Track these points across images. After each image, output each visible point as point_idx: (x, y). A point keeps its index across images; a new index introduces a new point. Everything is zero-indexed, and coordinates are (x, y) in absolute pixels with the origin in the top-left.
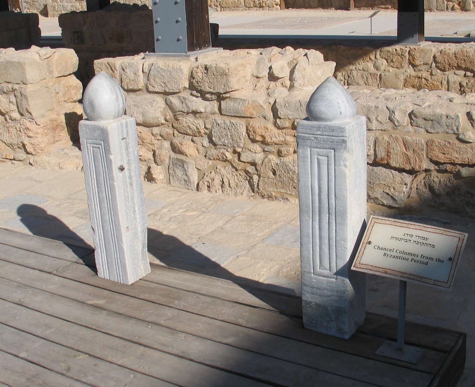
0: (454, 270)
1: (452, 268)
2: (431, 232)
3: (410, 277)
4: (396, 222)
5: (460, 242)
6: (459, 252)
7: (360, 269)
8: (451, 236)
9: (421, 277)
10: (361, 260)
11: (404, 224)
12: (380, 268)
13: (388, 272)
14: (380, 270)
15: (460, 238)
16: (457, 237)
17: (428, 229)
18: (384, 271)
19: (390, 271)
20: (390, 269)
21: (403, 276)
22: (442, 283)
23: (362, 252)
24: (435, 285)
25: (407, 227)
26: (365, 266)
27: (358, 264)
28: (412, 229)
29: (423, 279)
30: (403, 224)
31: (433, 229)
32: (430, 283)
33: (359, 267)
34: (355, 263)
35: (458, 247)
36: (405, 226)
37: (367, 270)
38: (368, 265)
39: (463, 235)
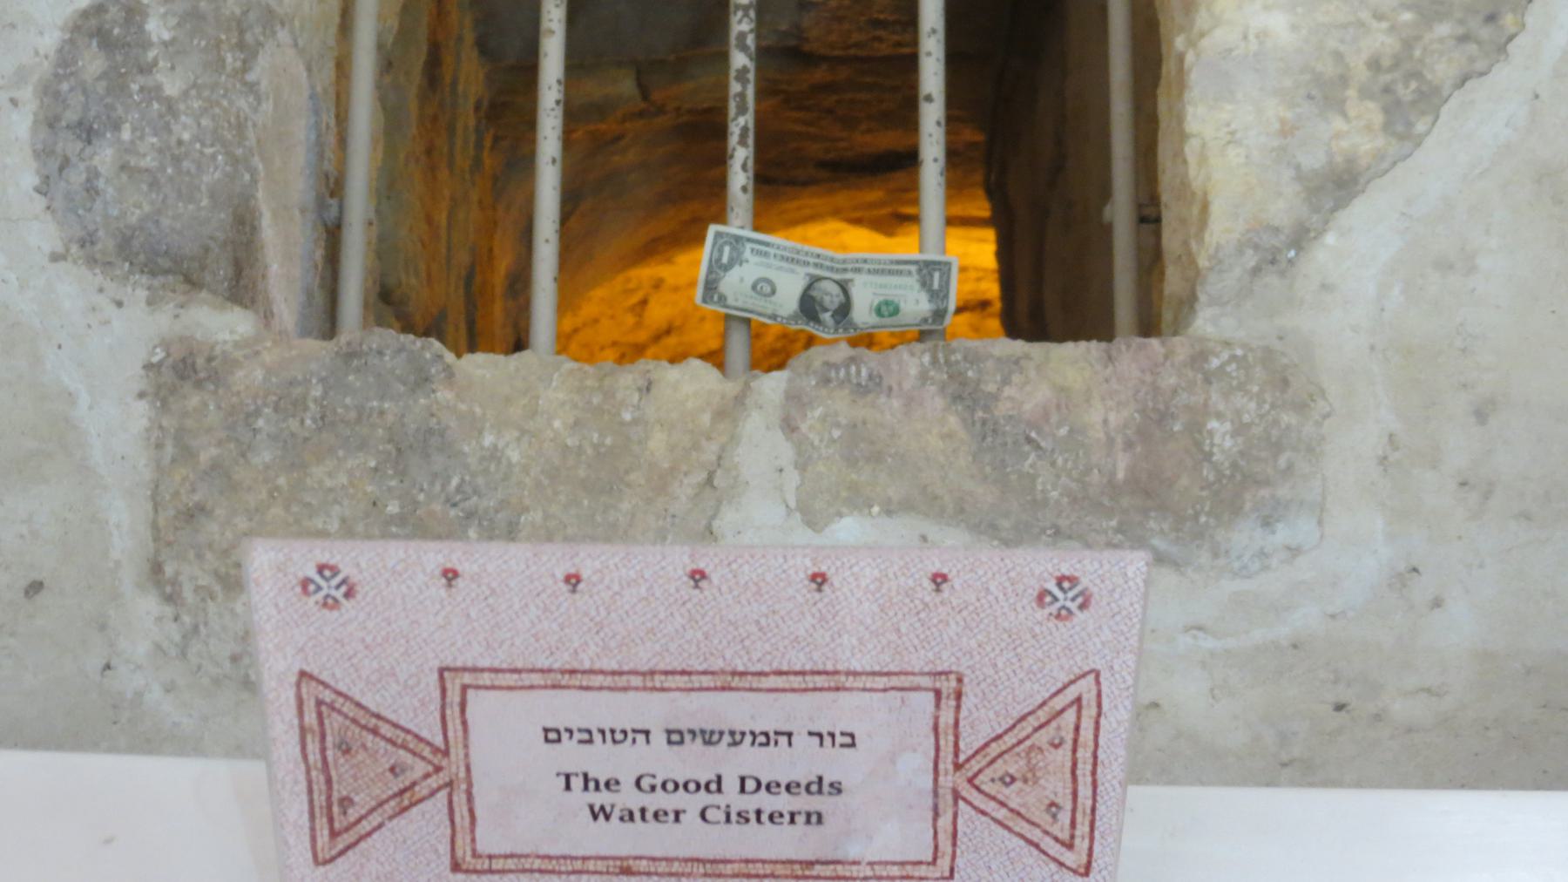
8: (893, 688)
9: (801, 863)
10: (473, 840)
19: (644, 862)
20: (640, 858)
25: (649, 684)
30: (625, 678)
31: (792, 678)
39: (952, 677)
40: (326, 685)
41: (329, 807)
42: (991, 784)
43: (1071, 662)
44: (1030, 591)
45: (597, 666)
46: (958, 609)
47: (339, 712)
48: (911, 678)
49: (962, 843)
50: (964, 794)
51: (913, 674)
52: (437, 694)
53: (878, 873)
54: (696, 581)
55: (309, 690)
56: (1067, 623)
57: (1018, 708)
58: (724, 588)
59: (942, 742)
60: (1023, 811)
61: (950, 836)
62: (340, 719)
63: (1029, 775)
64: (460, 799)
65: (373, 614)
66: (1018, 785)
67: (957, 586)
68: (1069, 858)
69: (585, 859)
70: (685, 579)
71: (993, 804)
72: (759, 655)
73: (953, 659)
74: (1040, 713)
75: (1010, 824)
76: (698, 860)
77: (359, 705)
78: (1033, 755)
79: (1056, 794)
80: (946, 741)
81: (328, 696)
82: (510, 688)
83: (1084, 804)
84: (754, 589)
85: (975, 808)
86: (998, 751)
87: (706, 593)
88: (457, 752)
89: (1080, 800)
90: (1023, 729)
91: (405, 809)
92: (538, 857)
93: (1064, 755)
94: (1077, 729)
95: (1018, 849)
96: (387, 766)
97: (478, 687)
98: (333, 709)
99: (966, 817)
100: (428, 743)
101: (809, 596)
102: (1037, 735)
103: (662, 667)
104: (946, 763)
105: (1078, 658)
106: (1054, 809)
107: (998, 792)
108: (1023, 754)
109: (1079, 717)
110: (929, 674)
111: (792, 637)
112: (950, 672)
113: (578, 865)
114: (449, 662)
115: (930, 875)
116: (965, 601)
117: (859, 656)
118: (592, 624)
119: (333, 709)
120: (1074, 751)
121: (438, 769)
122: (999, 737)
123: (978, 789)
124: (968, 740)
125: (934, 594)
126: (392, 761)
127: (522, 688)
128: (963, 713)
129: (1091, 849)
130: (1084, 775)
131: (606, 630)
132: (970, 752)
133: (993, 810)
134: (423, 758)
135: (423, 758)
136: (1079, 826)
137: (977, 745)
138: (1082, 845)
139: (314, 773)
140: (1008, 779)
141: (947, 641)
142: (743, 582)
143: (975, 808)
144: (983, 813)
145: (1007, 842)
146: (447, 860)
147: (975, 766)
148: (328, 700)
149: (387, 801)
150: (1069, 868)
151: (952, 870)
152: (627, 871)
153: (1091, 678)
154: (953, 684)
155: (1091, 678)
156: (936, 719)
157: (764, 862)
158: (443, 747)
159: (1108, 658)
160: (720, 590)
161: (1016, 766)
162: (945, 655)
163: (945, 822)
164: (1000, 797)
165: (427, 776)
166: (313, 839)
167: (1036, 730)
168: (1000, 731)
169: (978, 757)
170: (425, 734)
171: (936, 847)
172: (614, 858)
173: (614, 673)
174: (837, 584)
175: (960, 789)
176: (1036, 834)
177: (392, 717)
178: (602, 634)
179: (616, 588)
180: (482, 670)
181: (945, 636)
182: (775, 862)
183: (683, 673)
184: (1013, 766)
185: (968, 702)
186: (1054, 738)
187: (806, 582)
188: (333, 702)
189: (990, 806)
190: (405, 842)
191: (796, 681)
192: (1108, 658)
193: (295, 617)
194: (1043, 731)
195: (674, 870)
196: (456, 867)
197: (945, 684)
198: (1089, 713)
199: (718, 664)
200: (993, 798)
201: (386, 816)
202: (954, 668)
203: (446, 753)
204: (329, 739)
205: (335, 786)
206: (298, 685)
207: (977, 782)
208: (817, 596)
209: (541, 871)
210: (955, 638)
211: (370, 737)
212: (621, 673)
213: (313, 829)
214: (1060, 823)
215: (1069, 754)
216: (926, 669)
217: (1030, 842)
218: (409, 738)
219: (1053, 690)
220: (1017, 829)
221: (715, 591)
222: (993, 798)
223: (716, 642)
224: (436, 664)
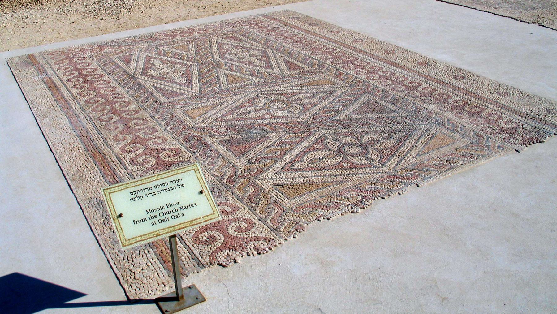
2: (168, 177)
3: (182, 227)
4: (130, 183)
7: (131, 246)
8: (186, 171)
9: (190, 221)
10: (124, 236)
12: (149, 234)
13: (159, 234)
14: (150, 236)
15: (195, 170)
16: (192, 170)
18: (155, 234)
20: (159, 230)
21: (175, 229)
22: (210, 216)
23: (120, 228)
24: (206, 221)
25: (143, 183)
26: (133, 240)
27: (125, 242)
28: (149, 182)
29: (193, 222)
33: (128, 244)
34: (122, 242)
35: (199, 178)
38: (136, 237)
48: (188, 168)
82: (118, 191)
92: (139, 237)
97: (112, 193)
127: (120, 190)
171: (212, 209)
172: (154, 232)
197: (195, 168)
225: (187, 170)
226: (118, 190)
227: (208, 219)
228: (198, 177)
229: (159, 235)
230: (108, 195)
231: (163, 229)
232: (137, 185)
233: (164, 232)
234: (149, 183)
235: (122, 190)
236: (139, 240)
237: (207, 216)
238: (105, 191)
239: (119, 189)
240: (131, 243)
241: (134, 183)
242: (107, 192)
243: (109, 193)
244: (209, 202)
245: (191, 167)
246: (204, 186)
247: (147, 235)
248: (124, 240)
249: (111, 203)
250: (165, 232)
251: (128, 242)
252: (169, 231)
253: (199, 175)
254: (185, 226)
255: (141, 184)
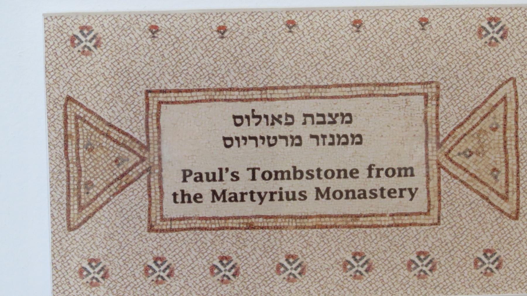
0: (436, 179)
1: (431, 173)
3: (324, 224)
4: (227, 90)
5: (429, 105)
6: (434, 130)
8: (400, 94)
9: (351, 216)
10: (161, 208)
11: (254, 92)
12: (229, 218)
13: (256, 225)
15: (426, 96)
16: (419, 94)
17: (328, 90)
19: (261, 220)
20: (259, 217)
21: (303, 225)
22: (414, 217)
25: (264, 96)
26: (182, 222)
27: (158, 222)
29: (361, 219)
30: (250, 92)
31: (344, 89)
32: (383, 223)
33: (164, 227)
34: (149, 221)
35: (429, 118)
36: (259, 97)
37: (192, 231)
39: (434, 85)
40: (82, 106)
41: (79, 188)
42: (458, 157)
43: (499, 73)
44: (474, 28)
45: (235, 86)
46: (434, 41)
47: (89, 124)
48: (410, 87)
49: (444, 198)
50: (443, 164)
51: (412, 84)
52: (143, 109)
53: (396, 222)
54: (290, 28)
55: (72, 108)
56: (495, 48)
57: (472, 104)
58: (306, 32)
59: (430, 129)
60: (478, 175)
61: (437, 194)
62: (88, 127)
63: (480, 150)
64: (154, 180)
65: (110, 56)
66: (474, 156)
67: (433, 26)
68: (506, 207)
69: (227, 218)
70: (284, 26)
71: (460, 171)
72: (326, 74)
73: (433, 74)
74: (484, 107)
75: (471, 184)
76: (292, 217)
77: (99, 118)
78: (481, 136)
79: (495, 162)
80: (432, 128)
81: (82, 112)
83: (512, 169)
84: (322, 31)
85: (450, 173)
86: (462, 134)
87: (296, 35)
88: (153, 148)
89: (510, 166)
90: (475, 118)
91: (123, 188)
93: (499, 133)
94: (505, 117)
95: (476, 202)
96: (114, 159)
97: (167, 103)
98: (85, 121)
99: (446, 180)
100: (138, 142)
101: (352, 35)
102: (483, 122)
103: (271, 84)
104: (432, 145)
105: (503, 70)
106: (495, 173)
107: (463, 162)
108: (476, 136)
109: (505, 110)
110: (419, 83)
111: (344, 62)
112: (432, 82)
113: (222, 223)
114: (151, 87)
115: (427, 222)
116: (438, 36)
117: (381, 73)
118: (232, 58)
119: (85, 121)
120: (505, 133)
121: (143, 159)
122: (462, 124)
123: (451, 160)
124: (444, 127)
125: (421, 31)
126: (117, 155)
127: (192, 102)
128: (441, 109)
129: (518, 200)
130: (511, 149)
131: (240, 61)
132: (445, 135)
133: (461, 175)
134: (135, 152)
135: (135, 152)
136: (510, 185)
137: (449, 130)
138: (513, 197)
139: (71, 165)
140: (468, 153)
141: (430, 62)
142: (316, 27)
143: (450, 173)
144: (456, 177)
145: (470, 197)
146: (145, 223)
147: (449, 144)
148: (82, 115)
149: (112, 184)
150: (505, 214)
151: (439, 218)
152: (251, 227)
153: (511, 82)
154: (434, 90)
155: (511, 82)
156: (426, 113)
157: (330, 216)
158: (146, 144)
159: (520, 70)
160: (303, 33)
161: (472, 144)
162: (429, 71)
163: (433, 183)
164: (464, 165)
165: (136, 164)
166: (68, 211)
167: (482, 119)
168: (462, 121)
169: (450, 139)
170: (136, 135)
171: (429, 202)
172: (243, 217)
173: (244, 90)
174: (367, 27)
175: (440, 161)
176: (486, 191)
177: (118, 125)
178: (238, 64)
179: (246, 34)
180: (170, 91)
181: (428, 59)
182: (336, 216)
183: (283, 88)
184: (470, 144)
185: (443, 101)
186: (493, 124)
187: (351, 26)
188: (85, 116)
189: (458, 172)
190: (122, 211)
191: (346, 91)
192: (520, 70)
193: (66, 61)
194: (486, 120)
195: (278, 224)
196: (151, 228)
197: (430, 90)
198: (511, 106)
199: (303, 81)
200: (460, 167)
201: (111, 193)
202: (434, 79)
203: (147, 148)
204: (81, 141)
205: (83, 174)
206: (65, 106)
207: (450, 155)
208: (357, 35)
209: (200, 229)
210: (434, 60)
211: (105, 139)
212: (248, 90)
213: (68, 205)
214: (499, 182)
215: (502, 134)
216: (419, 81)
217: (482, 196)
218: (127, 139)
219: (490, 92)
220: (475, 187)
221: (300, 33)
222: (460, 167)
223: (301, 66)
224: (144, 88)
225: (404, 91)
226: (187, 99)
227: (404, 222)
228: (426, 117)
229: (254, 228)
230: (155, 107)
231: (271, 217)
232: (243, 98)
233: (270, 225)
234: (280, 101)
235: (197, 101)
236: (197, 226)
237: (406, 215)
238: (150, 95)
239: (191, 99)
240: (173, 227)
241: (237, 93)
242: (156, 99)
243: (160, 103)
244: (428, 183)
245: (419, 86)
246: (434, 141)
247: (223, 221)
248: (159, 218)
249: (155, 126)
250: (274, 224)
251: (167, 225)
252: (286, 224)
253: (434, 111)
254: (333, 223)
255: (256, 100)
